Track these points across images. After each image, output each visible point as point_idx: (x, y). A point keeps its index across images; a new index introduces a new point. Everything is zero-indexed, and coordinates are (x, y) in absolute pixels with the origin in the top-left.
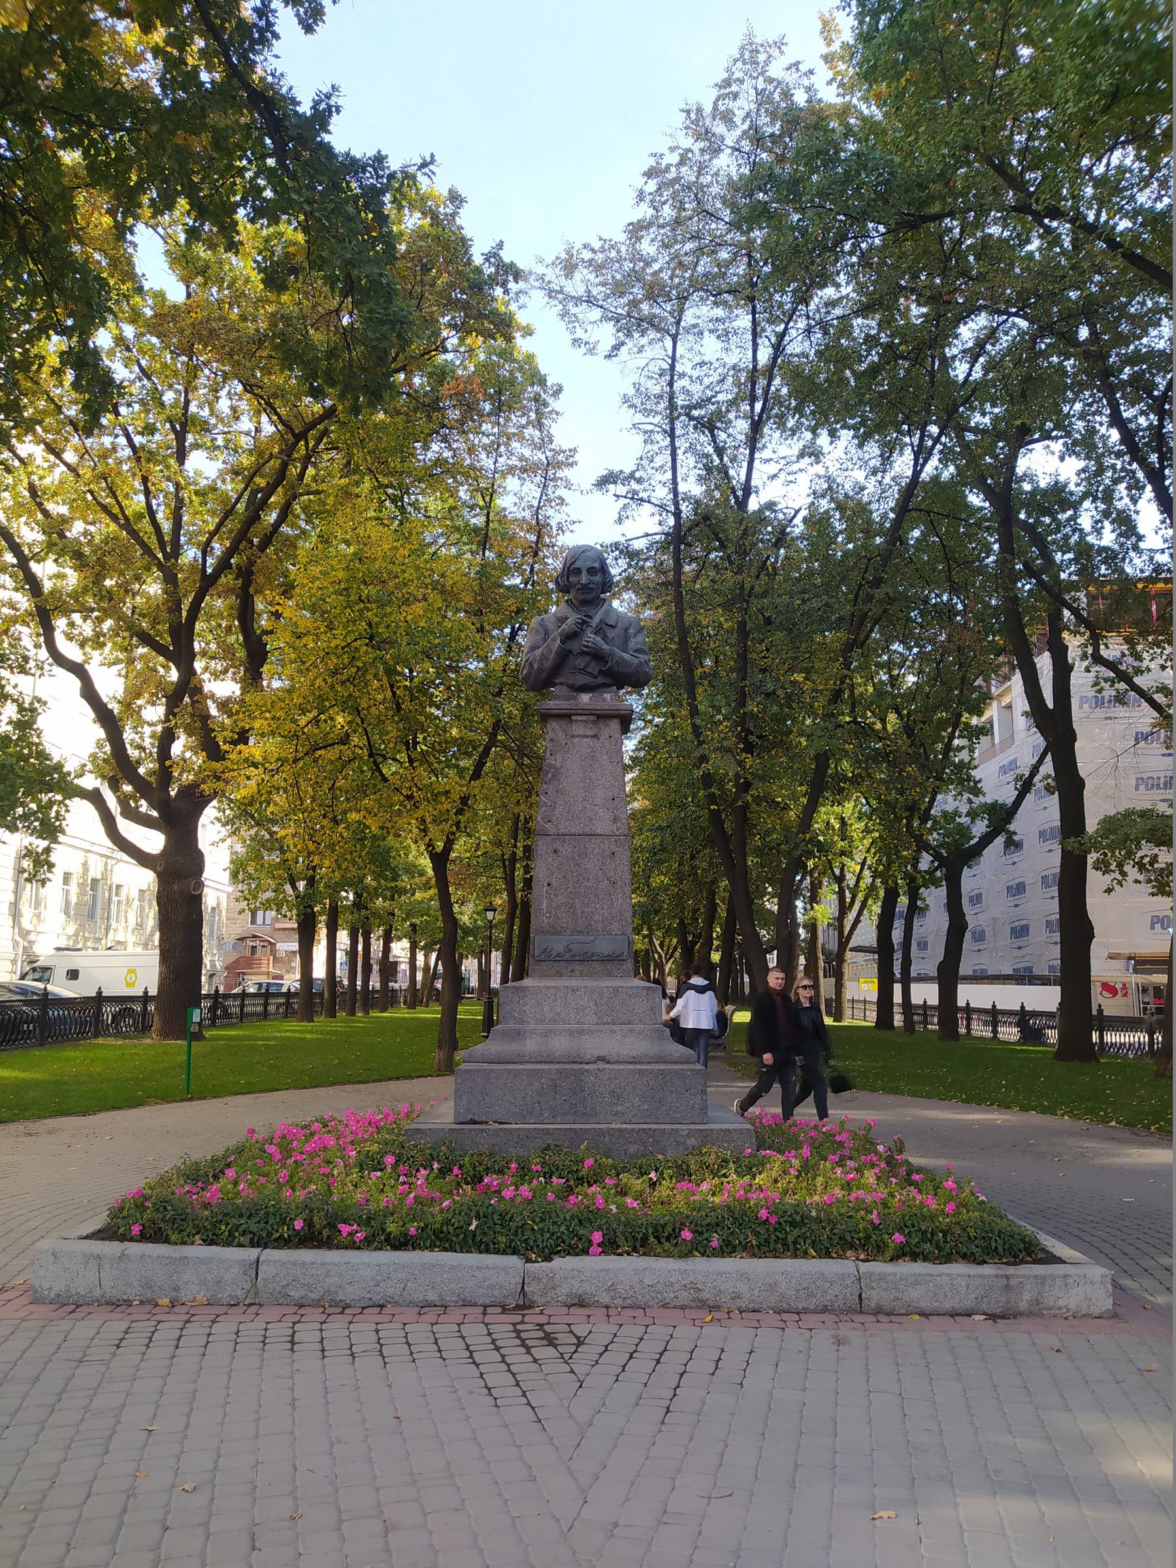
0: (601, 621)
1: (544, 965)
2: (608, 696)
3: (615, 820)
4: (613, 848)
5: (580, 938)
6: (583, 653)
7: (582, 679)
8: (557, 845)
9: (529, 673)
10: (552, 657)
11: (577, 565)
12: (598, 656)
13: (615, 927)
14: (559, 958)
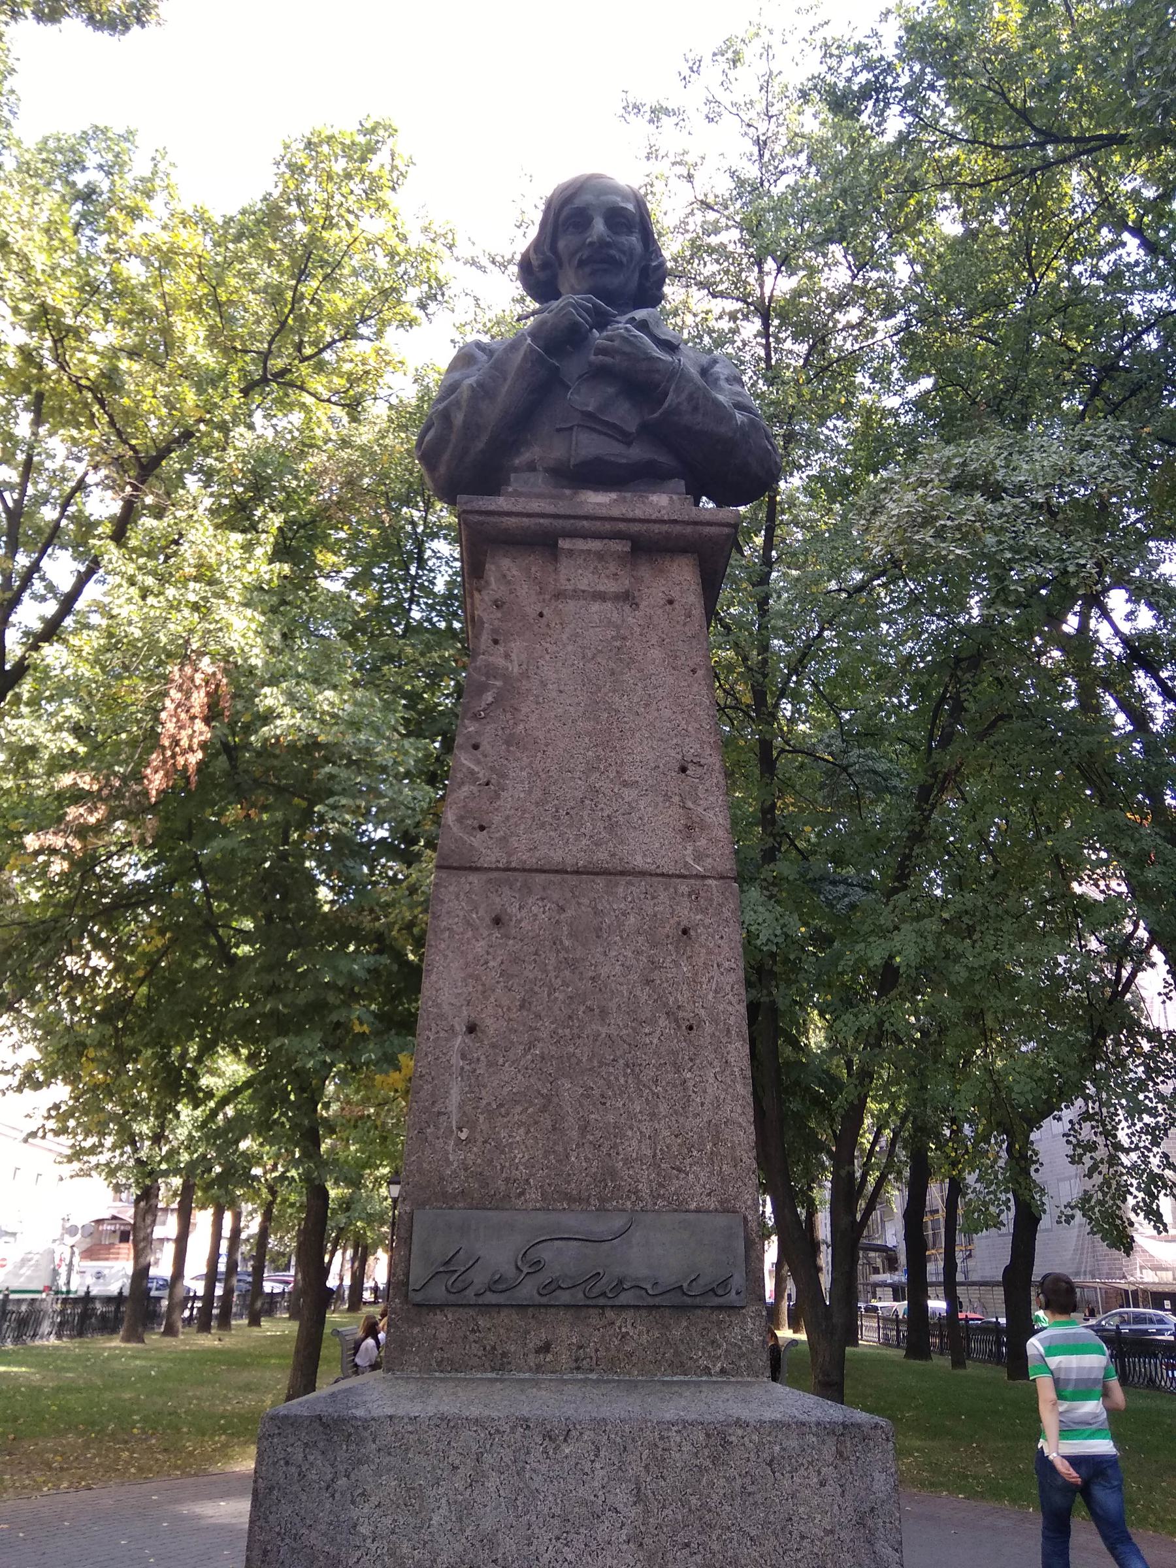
1: (442, 1325)
3: (690, 829)
4: (686, 913)
5: (573, 1221)
6: (600, 373)
8: (507, 900)
13: (698, 1184)
14: (495, 1300)
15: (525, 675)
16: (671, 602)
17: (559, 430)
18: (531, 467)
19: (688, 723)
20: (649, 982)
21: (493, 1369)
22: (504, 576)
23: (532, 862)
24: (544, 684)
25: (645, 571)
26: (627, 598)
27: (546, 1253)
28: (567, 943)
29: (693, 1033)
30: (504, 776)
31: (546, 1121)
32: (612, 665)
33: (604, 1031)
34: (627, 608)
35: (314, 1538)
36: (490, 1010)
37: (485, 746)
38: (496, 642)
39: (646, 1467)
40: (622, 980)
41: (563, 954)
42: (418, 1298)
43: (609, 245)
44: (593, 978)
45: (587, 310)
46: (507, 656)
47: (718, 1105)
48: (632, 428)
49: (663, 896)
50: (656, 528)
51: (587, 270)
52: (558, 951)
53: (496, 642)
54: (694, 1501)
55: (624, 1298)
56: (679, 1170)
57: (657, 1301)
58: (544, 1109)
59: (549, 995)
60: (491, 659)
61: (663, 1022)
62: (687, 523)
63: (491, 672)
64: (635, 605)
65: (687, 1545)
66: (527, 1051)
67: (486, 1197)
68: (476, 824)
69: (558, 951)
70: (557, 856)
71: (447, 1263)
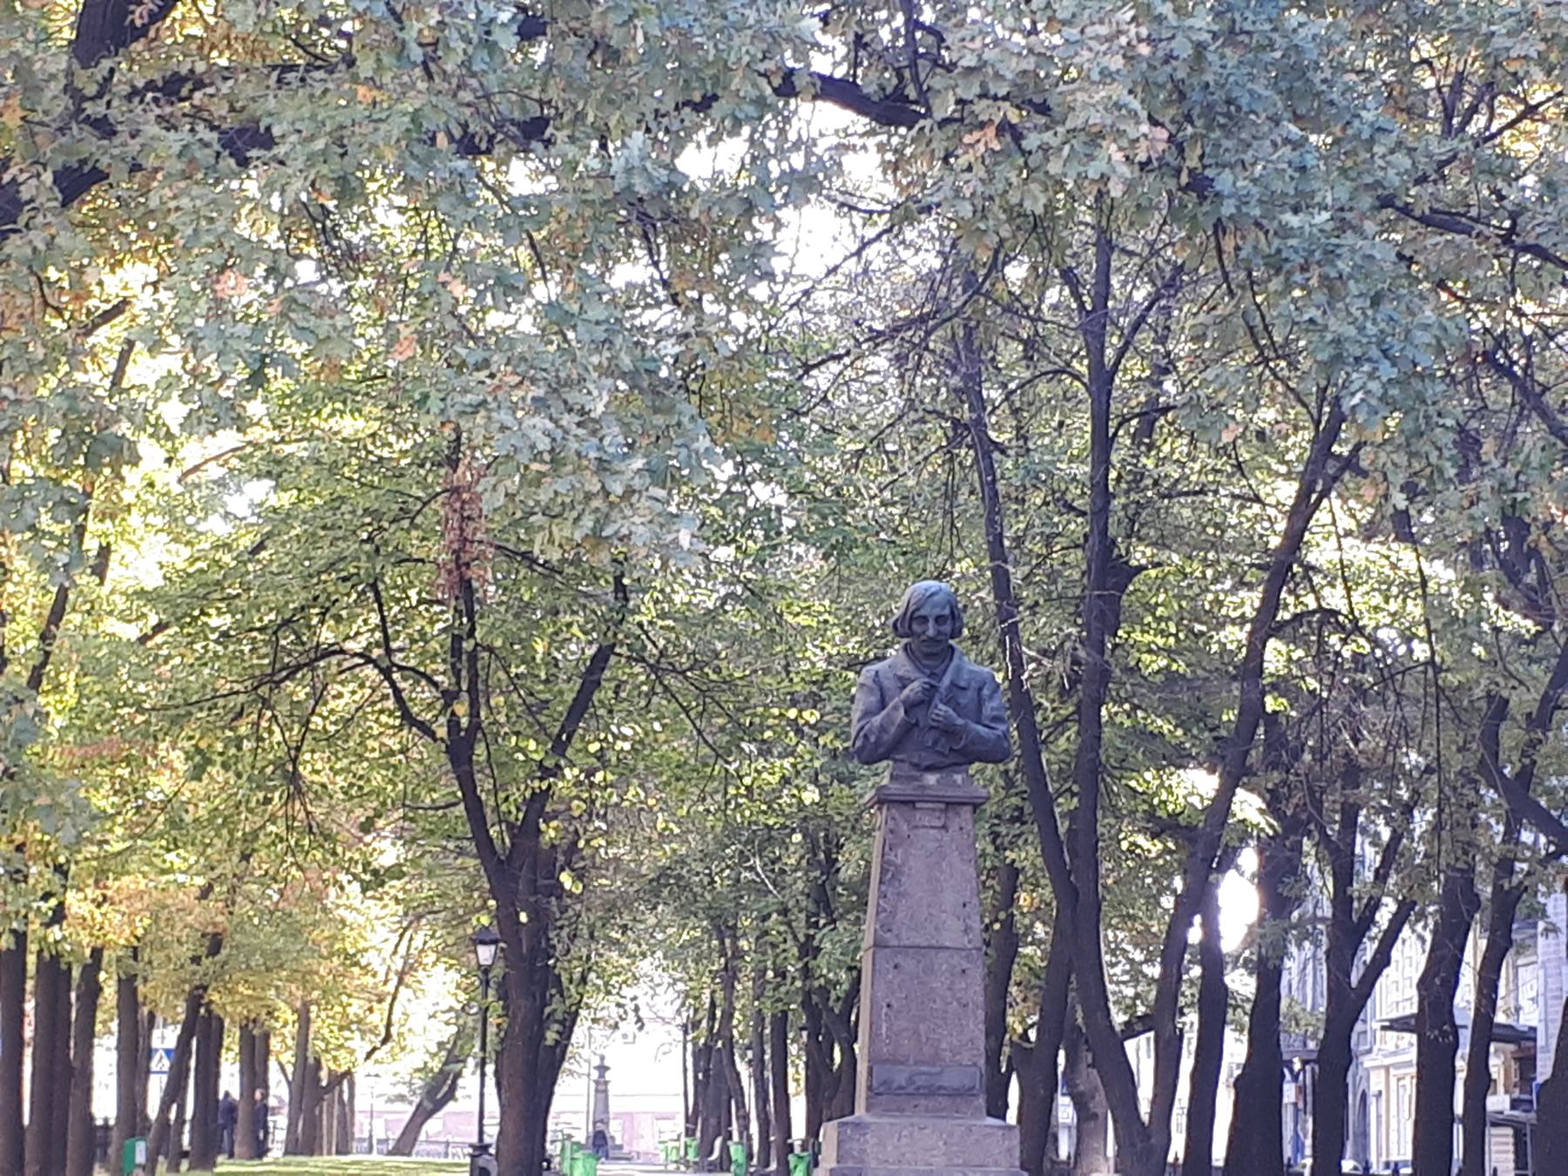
0: (953, 684)
3: (966, 930)
4: (965, 965)
8: (899, 959)
10: (893, 730)
11: (922, 612)
12: (948, 731)
13: (965, 1058)
26: (944, 827)
63: (890, 863)
67: (896, 1061)
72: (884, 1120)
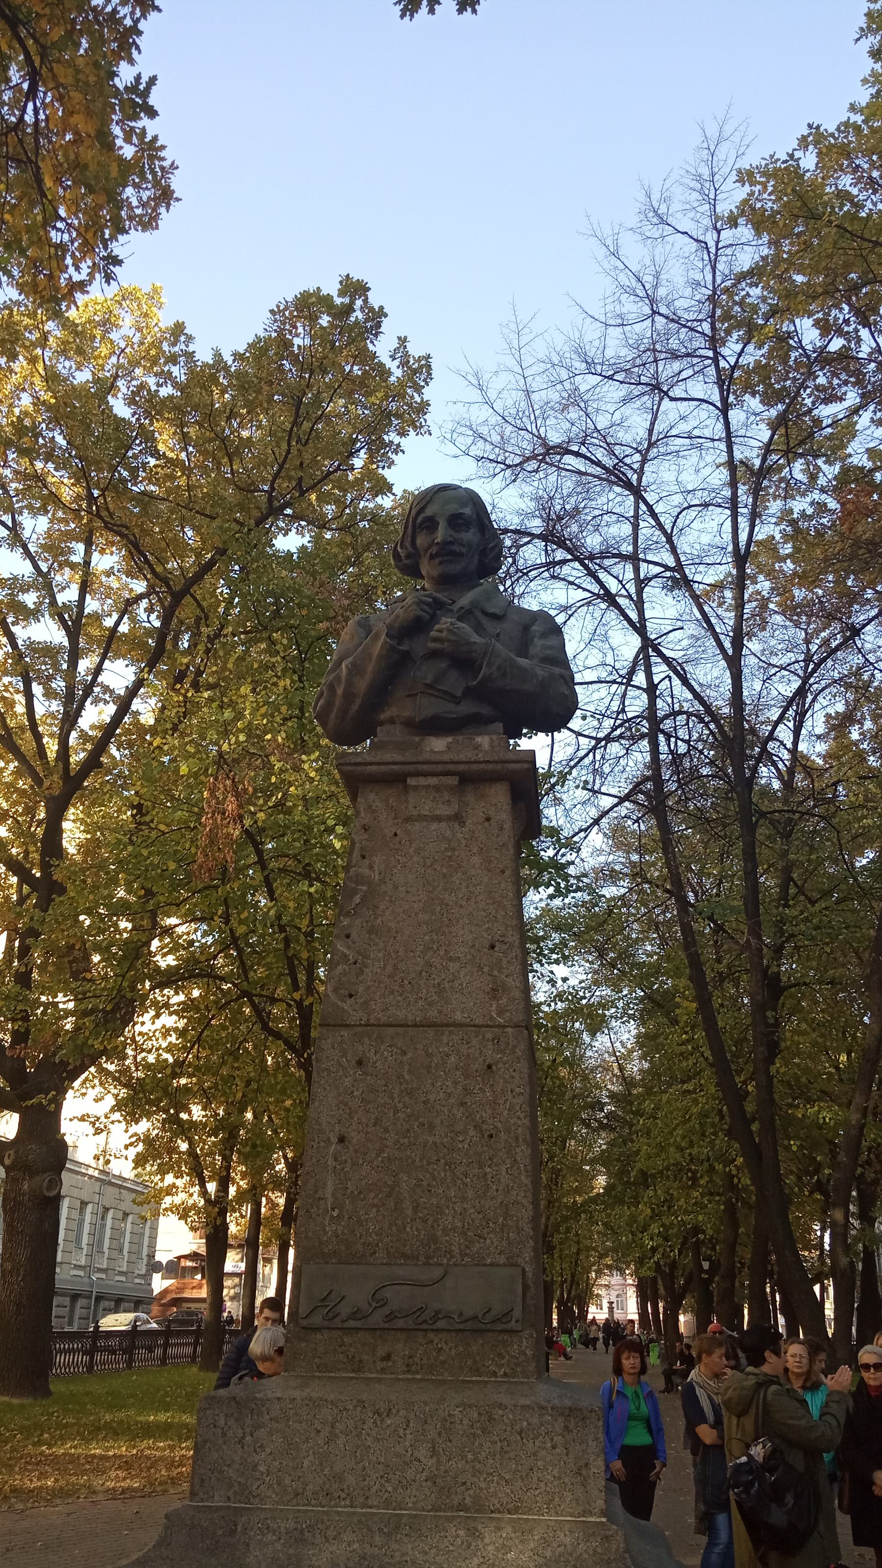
0: (474, 604)
2: (484, 741)
3: (495, 992)
4: (490, 1055)
6: (434, 654)
7: (430, 707)
9: (329, 705)
10: (370, 669)
11: (429, 512)
12: (463, 661)
15: (383, 881)
16: (488, 819)
17: (408, 696)
18: (392, 721)
19: (497, 911)
20: (463, 1104)
21: (353, 1371)
22: (370, 807)
23: (384, 1019)
24: (396, 888)
25: (470, 797)
26: (458, 818)
27: (388, 1293)
28: (407, 1077)
29: (493, 1140)
30: (366, 957)
31: (391, 1204)
32: (445, 871)
33: (431, 1139)
34: (457, 826)
35: (231, 1472)
36: (354, 1127)
37: (354, 935)
38: (363, 857)
39: (440, 1434)
40: (444, 1103)
41: (404, 1086)
42: (305, 1323)
43: (451, 543)
44: (424, 1102)
45: (428, 604)
46: (371, 867)
47: (508, 1190)
48: (459, 693)
49: (474, 1042)
50: (475, 767)
51: (437, 561)
52: (401, 1084)
53: (363, 857)
54: (470, 1456)
55: (440, 1324)
56: (480, 1237)
57: (461, 1326)
58: (389, 1196)
59: (394, 1114)
60: (360, 870)
61: (472, 1132)
62: (497, 762)
63: (360, 880)
64: (462, 823)
65: (464, 1483)
66: (378, 1155)
68: (347, 993)
69: (401, 1084)
70: (401, 1014)
71: (324, 1300)
72: (315, 1390)
